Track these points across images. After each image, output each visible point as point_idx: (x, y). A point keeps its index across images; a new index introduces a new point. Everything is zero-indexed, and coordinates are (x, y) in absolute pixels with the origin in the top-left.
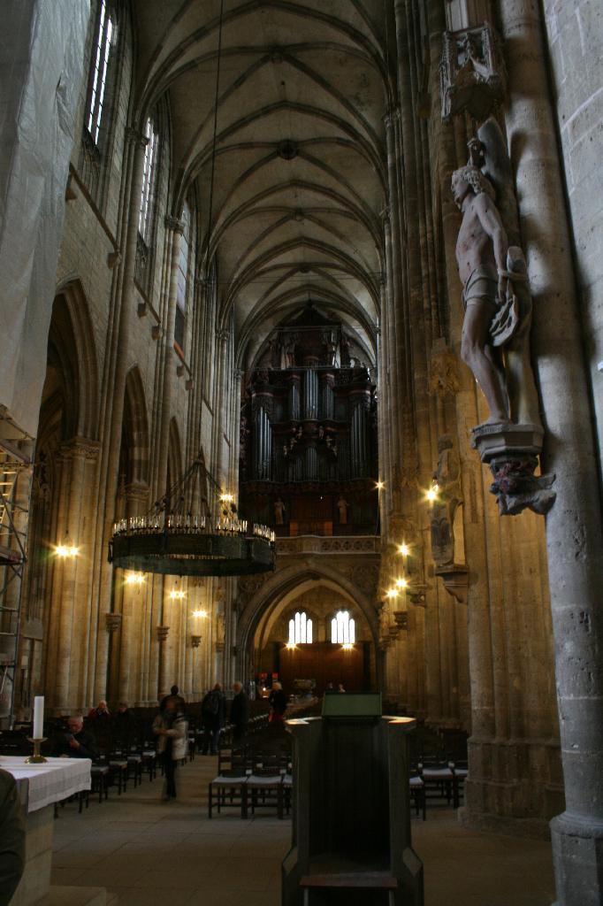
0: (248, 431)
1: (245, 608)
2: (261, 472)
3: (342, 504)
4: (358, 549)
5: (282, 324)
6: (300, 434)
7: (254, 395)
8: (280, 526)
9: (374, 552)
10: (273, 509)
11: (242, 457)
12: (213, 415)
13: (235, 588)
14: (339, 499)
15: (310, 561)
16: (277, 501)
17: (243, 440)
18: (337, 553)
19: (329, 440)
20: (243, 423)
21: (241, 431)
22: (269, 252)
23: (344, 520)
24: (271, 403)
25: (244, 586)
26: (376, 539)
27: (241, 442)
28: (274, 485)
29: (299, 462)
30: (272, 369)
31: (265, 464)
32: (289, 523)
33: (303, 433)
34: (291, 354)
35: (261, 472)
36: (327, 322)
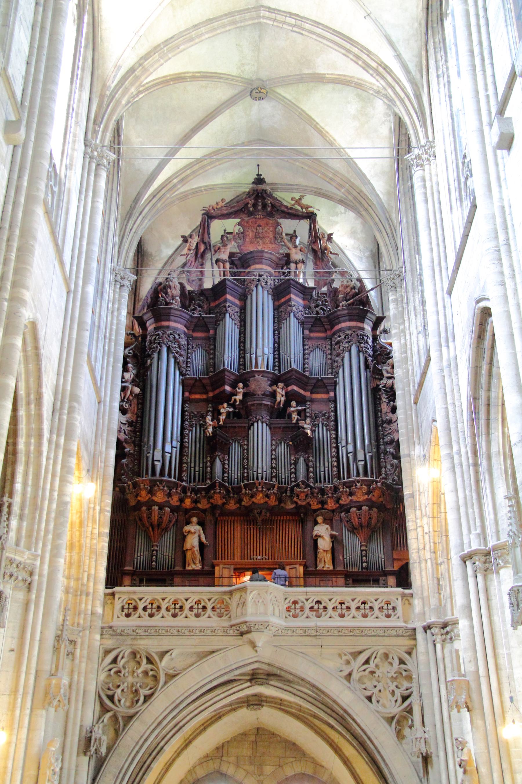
0: (137, 390)
1: (109, 749)
2: (158, 465)
3: (322, 530)
4: (365, 616)
5: (209, 216)
6: (239, 397)
7: (151, 326)
8: (195, 573)
9: (403, 624)
10: (182, 538)
11: (123, 437)
12: (68, 293)
13: (92, 697)
14: (316, 523)
15: (261, 639)
16: (188, 523)
17: (126, 406)
18: (319, 624)
19: (294, 407)
20: (127, 376)
21: (123, 389)
22: (196, 27)
23: (325, 563)
24: (183, 342)
25: (111, 698)
26: (403, 596)
27: (123, 411)
28: (184, 490)
29: (235, 449)
30: (188, 288)
31: (168, 448)
32: (213, 566)
33: (245, 395)
34: (224, 262)
35: (158, 465)
36: (291, 214)
